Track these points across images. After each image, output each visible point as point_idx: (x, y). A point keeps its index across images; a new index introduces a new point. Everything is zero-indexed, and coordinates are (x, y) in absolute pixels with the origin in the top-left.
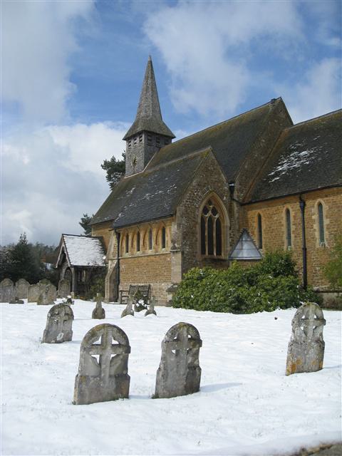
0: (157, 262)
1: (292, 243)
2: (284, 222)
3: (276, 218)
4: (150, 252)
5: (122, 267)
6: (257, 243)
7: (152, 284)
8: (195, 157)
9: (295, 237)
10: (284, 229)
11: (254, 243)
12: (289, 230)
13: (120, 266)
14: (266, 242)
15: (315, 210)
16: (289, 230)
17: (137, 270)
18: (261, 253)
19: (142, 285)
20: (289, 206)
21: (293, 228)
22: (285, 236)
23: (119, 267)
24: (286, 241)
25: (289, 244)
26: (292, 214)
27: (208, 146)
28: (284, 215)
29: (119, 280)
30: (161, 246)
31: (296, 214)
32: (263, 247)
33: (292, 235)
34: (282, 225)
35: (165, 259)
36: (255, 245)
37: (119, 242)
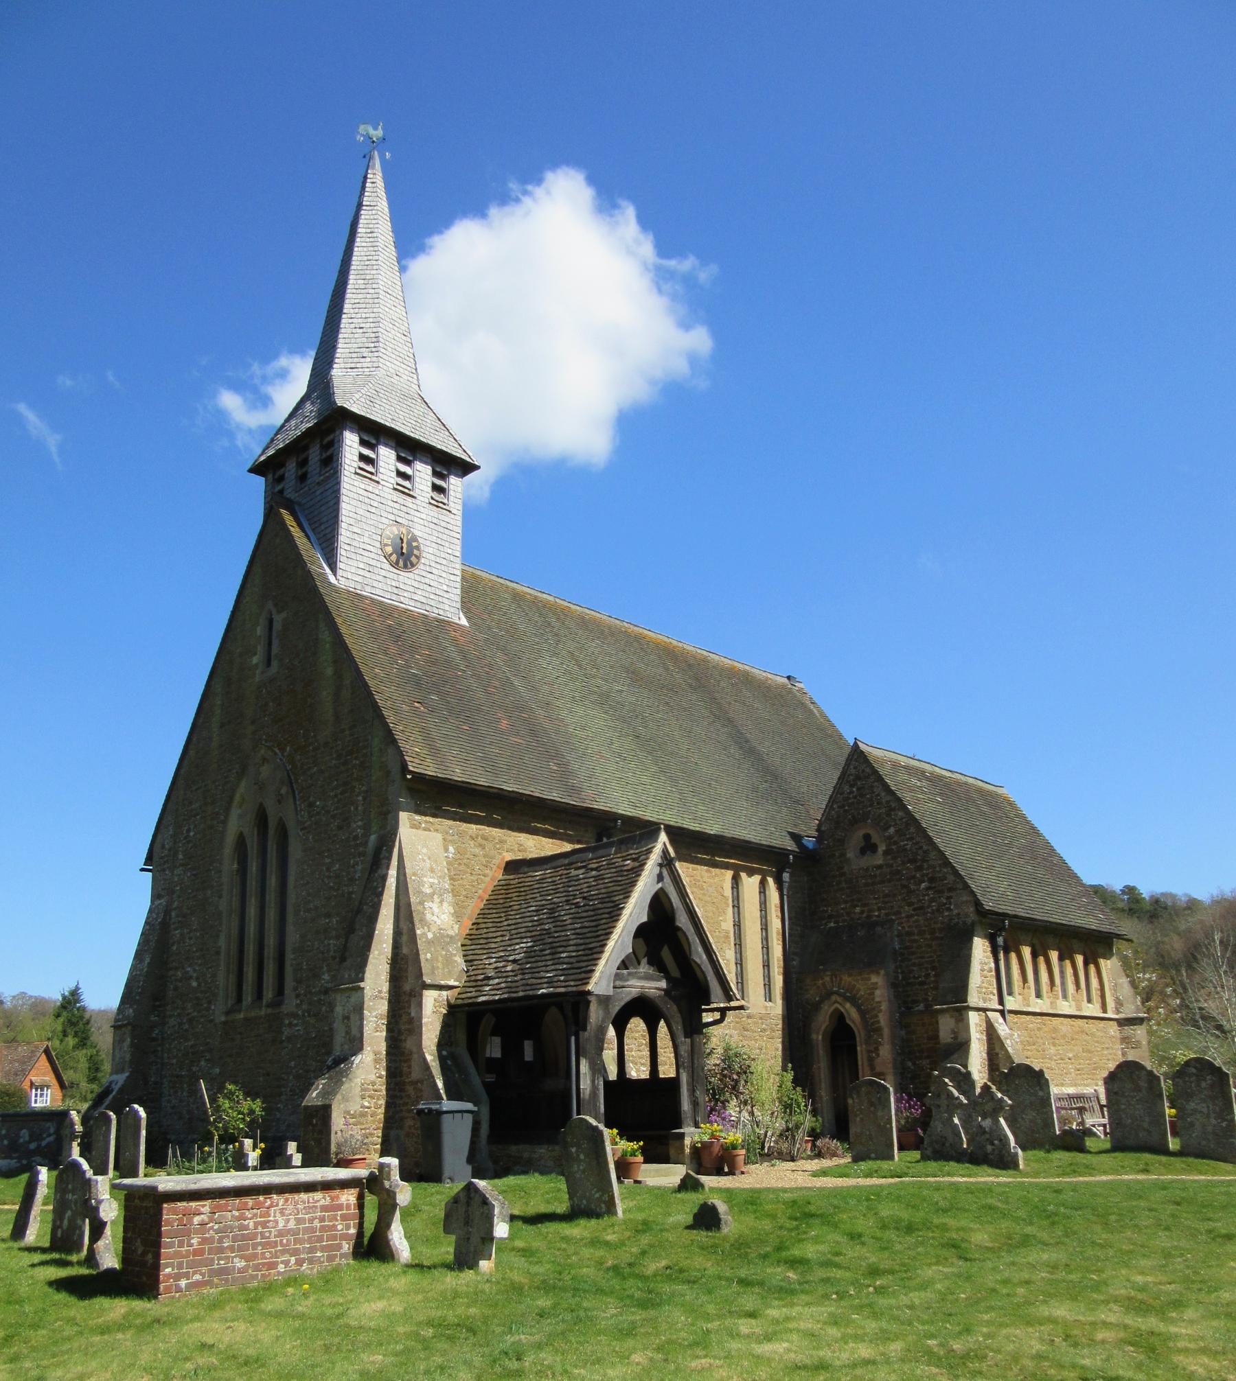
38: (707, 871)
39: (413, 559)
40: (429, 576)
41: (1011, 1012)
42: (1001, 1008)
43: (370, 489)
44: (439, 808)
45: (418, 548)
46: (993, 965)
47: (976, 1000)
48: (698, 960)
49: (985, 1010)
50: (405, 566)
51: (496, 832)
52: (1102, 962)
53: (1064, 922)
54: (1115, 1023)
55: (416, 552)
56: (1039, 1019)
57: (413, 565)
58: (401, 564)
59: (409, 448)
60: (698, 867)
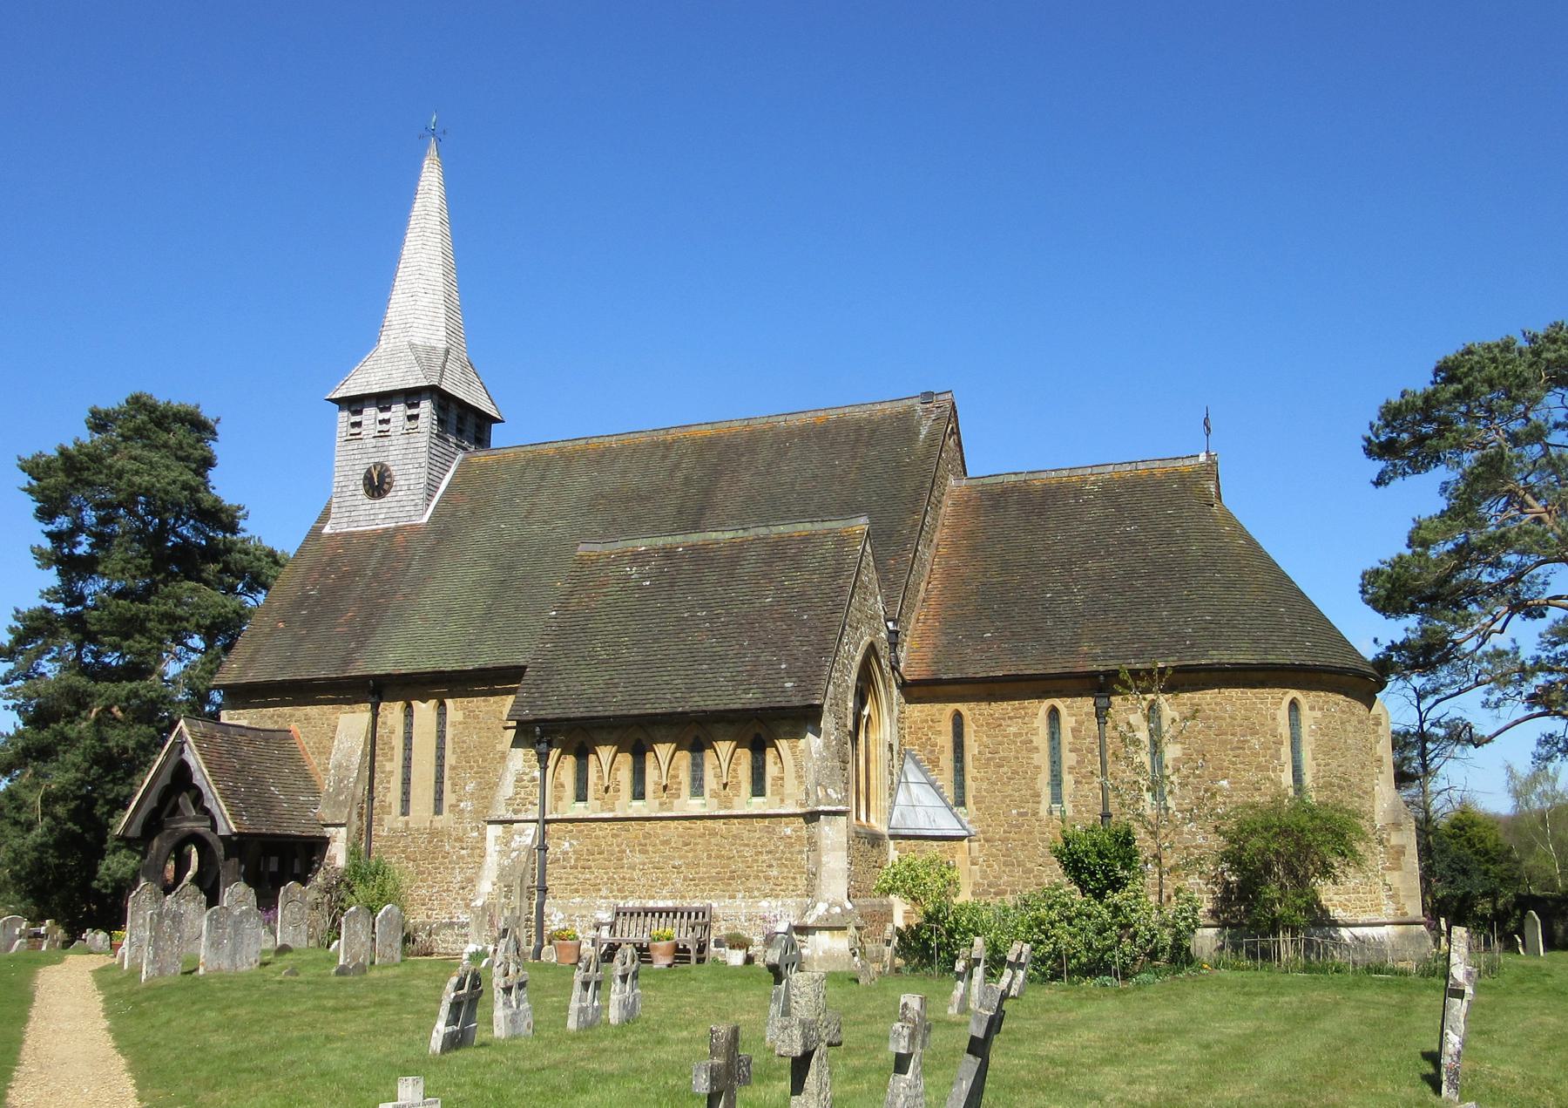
0: (735, 837)
1: (1066, 799)
2: (1041, 739)
3: (1013, 729)
4: (695, 806)
5: (562, 845)
6: (949, 792)
7: (715, 905)
8: (806, 539)
9: (1076, 782)
10: (1042, 759)
11: (938, 790)
12: (1056, 762)
13: (550, 843)
14: (978, 790)
15: (1137, 719)
16: (1056, 762)
17: (638, 858)
18: (965, 820)
19: (661, 904)
20: (1057, 702)
21: (1069, 759)
22: (1044, 778)
23: (543, 848)
24: (1046, 792)
25: (1057, 797)
26: (1067, 722)
27: (856, 511)
28: (1041, 723)
29: (544, 890)
30: (746, 787)
31: (1079, 723)
32: (970, 800)
33: (1068, 779)
34: (1037, 748)
35: (770, 832)
36: (940, 795)
37: (544, 769)
38: (484, 701)
39: (386, 487)
40: (400, 493)
41: (547, 822)
42: (537, 816)
43: (356, 447)
44: (248, 702)
45: (390, 476)
46: (537, 774)
47: (504, 812)
48: (209, 806)
49: (512, 822)
50: (380, 496)
51: (287, 710)
52: (783, 744)
53: (657, 711)
54: (801, 820)
55: (388, 480)
56: (619, 825)
57: (386, 492)
58: (376, 494)
59: (383, 400)
60: (475, 699)
